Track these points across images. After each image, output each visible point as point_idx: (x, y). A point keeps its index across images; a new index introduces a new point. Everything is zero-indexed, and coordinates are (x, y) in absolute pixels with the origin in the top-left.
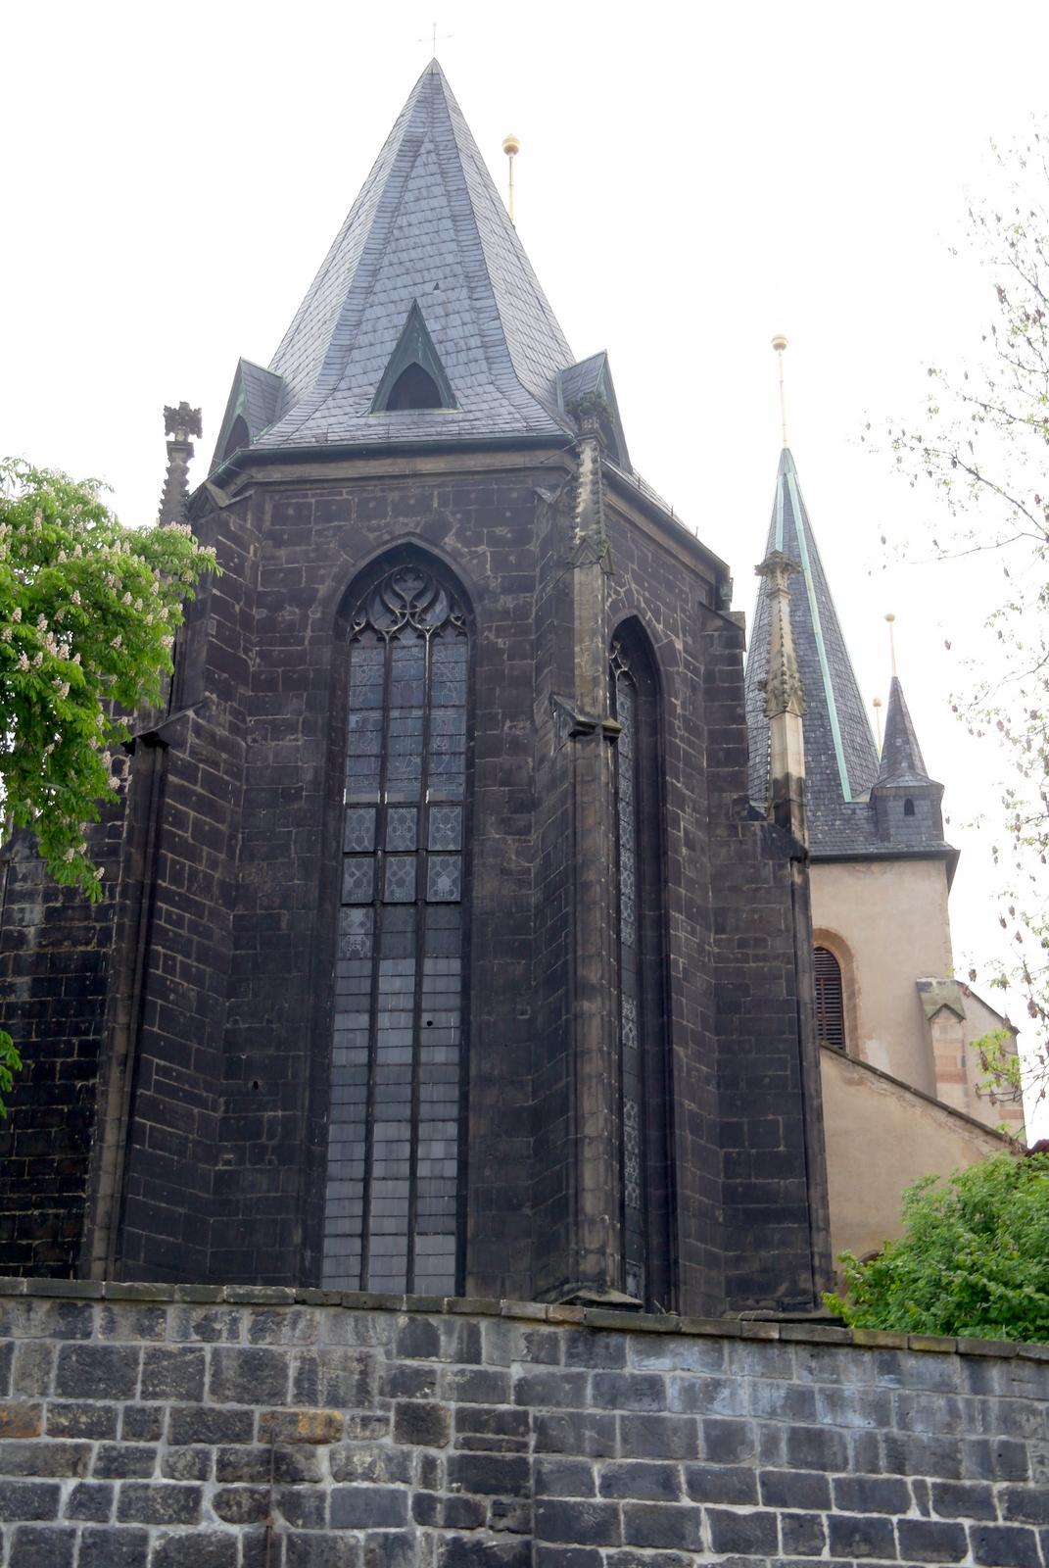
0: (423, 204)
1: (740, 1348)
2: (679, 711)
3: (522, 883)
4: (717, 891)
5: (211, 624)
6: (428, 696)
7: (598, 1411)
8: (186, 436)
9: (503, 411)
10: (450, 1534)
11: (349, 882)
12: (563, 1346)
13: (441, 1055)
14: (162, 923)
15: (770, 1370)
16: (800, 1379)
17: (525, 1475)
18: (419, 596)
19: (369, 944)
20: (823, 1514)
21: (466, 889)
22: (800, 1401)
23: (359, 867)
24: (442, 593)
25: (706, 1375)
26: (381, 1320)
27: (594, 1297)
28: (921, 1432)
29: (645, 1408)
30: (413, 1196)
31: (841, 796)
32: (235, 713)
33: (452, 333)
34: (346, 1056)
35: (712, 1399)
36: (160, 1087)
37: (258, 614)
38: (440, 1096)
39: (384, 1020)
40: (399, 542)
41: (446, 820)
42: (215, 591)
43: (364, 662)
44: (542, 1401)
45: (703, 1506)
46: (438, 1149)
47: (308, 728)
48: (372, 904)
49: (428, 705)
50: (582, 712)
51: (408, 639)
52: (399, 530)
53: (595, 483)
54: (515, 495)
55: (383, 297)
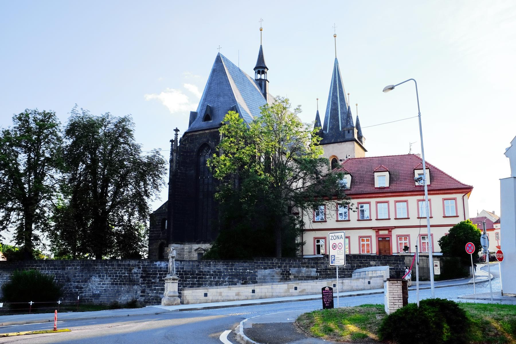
52: (204, 141)
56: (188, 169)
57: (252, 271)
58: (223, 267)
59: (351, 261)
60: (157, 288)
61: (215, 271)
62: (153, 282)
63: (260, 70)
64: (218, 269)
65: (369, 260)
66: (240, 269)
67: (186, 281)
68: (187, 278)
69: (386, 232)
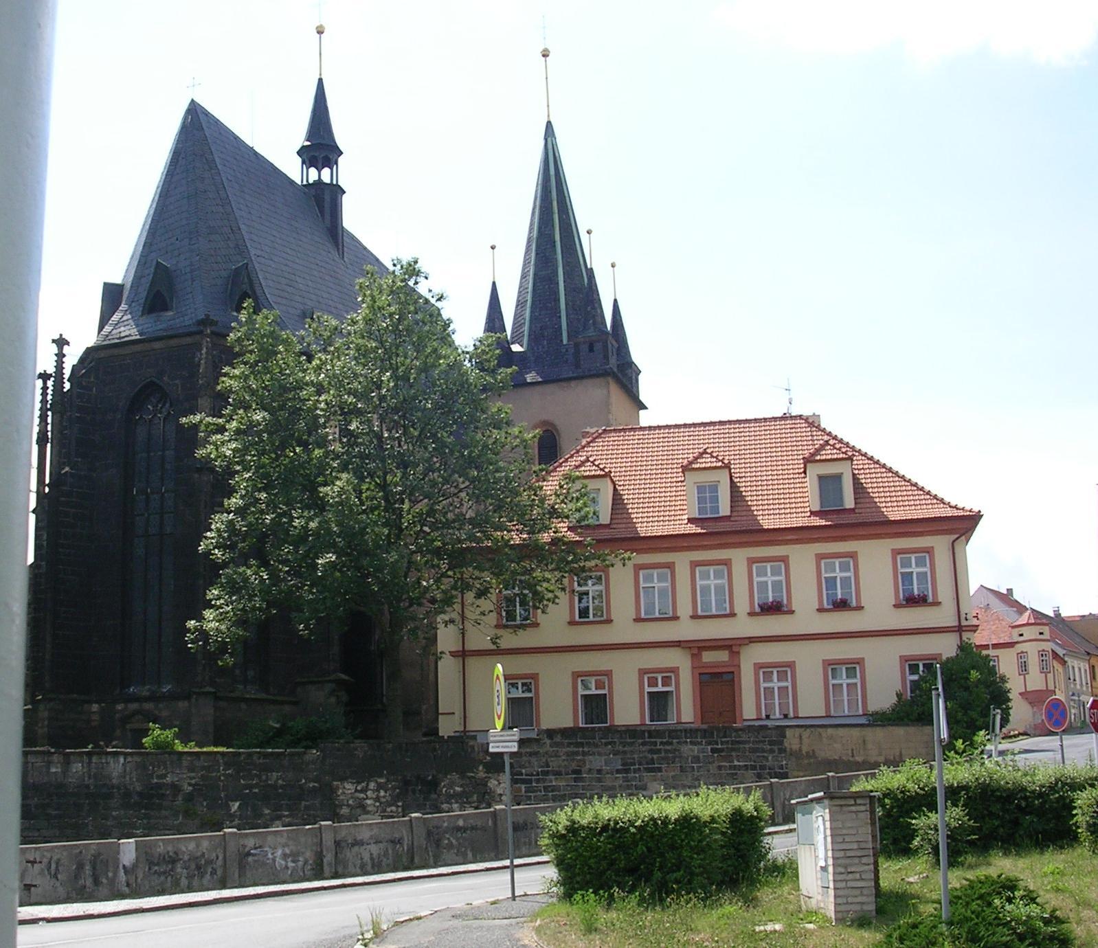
18: (159, 402)
27: (197, 690)
31: (562, 341)
43: (141, 433)
59: (624, 746)
65: (678, 743)
69: (723, 656)
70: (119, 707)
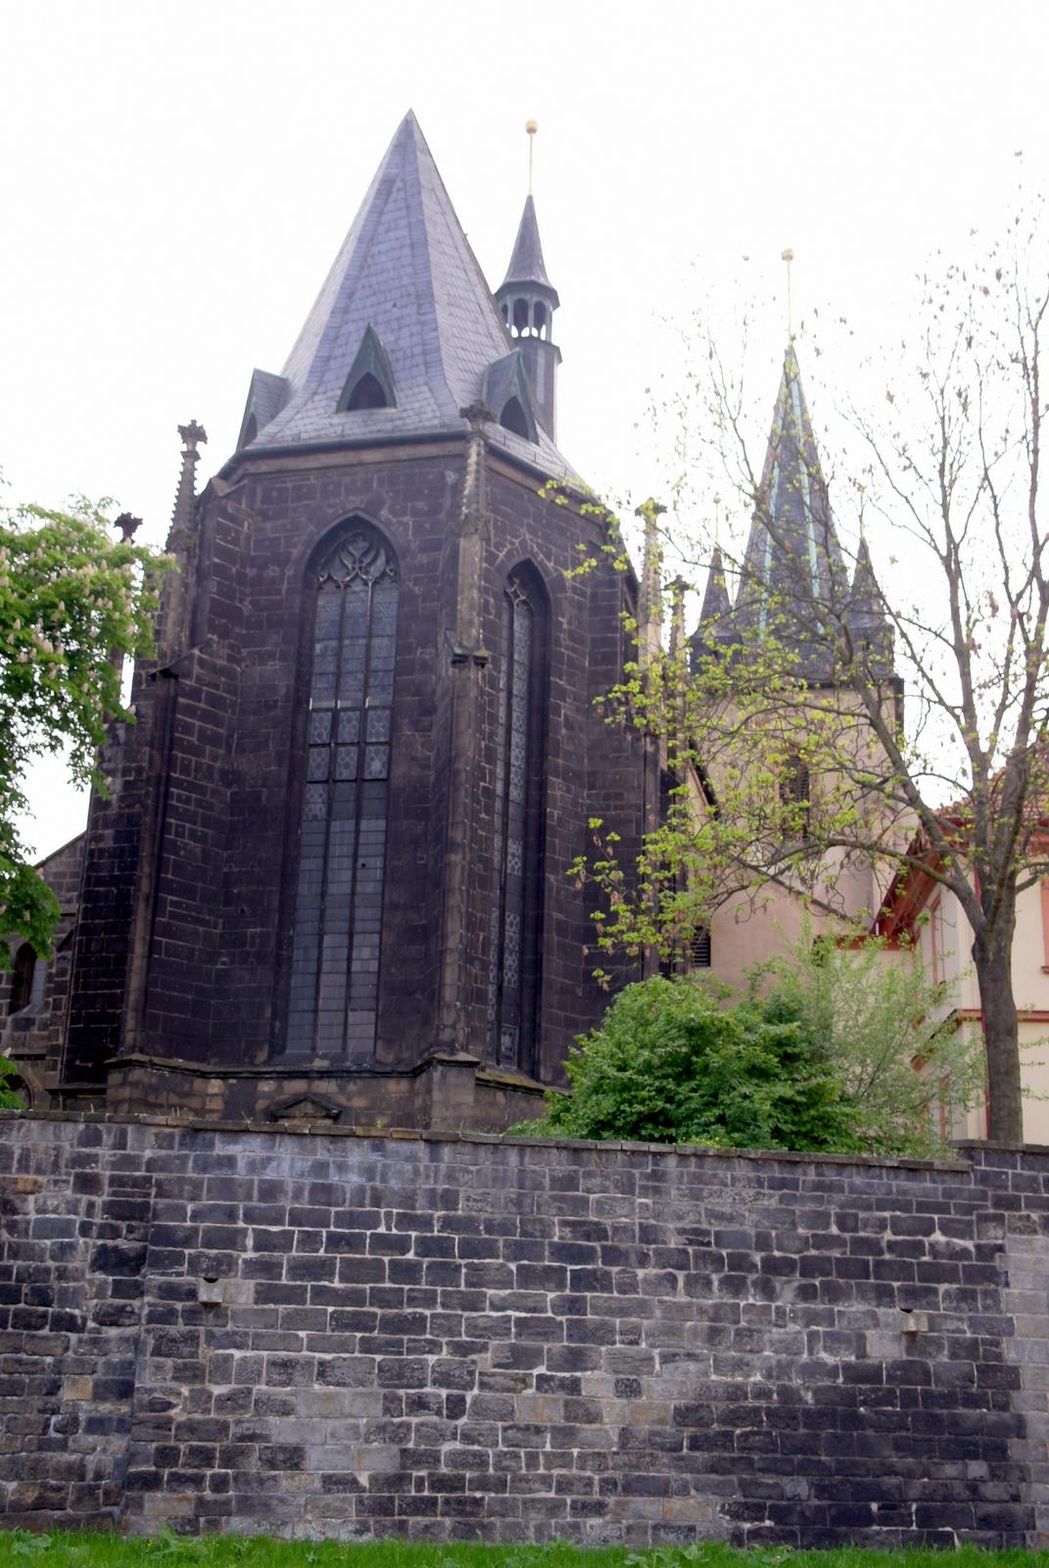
0: (392, 235)
1: (287, 1139)
2: (565, 626)
3: (425, 767)
4: (590, 759)
5: (212, 585)
6: (370, 629)
7: (195, 1175)
8: (194, 445)
9: (429, 409)
10: (100, 1242)
11: (312, 764)
12: (177, 1139)
13: (369, 887)
14: (174, 802)
15: (303, 1150)
16: (322, 1155)
17: (148, 1210)
18: (365, 554)
19: (324, 809)
20: (324, 1232)
21: (389, 773)
22: (320, 1168)
23: (319, 754)
24: (382, 552)
25: (264, 1154)
26: (70, 1127)
27: (445, 1057)
28: (394, 1184)
29: (224, 1173)
30: (349, 985)
32: (232, 647)
33: (403, 343)
34: (306, 889)
35: (265, 1168)
36: (172, 915)
37: (251, 572)
38: (367, 915)
39: (334, 863)
40: (350, 515)
41: (379, 720)
42: (216, 560)
43: (327, 605)
44: (161, 1170)
45: (250, 1227)
46: (366, 953)
47: (284, 657)
48: (327, 782)
49: (370, 635)
50: (461, 645)
51: (357, 587)
52: (350, 506)
53: (478, 471)
54: (431, 477)
55: (355, 315)
56: (244, 652)
57: (969, 1244)
58: (757, 1196)
60: (237, 1354)
61: (697, 1232)
62: (210, 1306)
63: (527, 297)
64: (720, 1217)
66: (882, 1225)
67: (473, 1304)
68: (477, 1277)
70: (266, 1087)
